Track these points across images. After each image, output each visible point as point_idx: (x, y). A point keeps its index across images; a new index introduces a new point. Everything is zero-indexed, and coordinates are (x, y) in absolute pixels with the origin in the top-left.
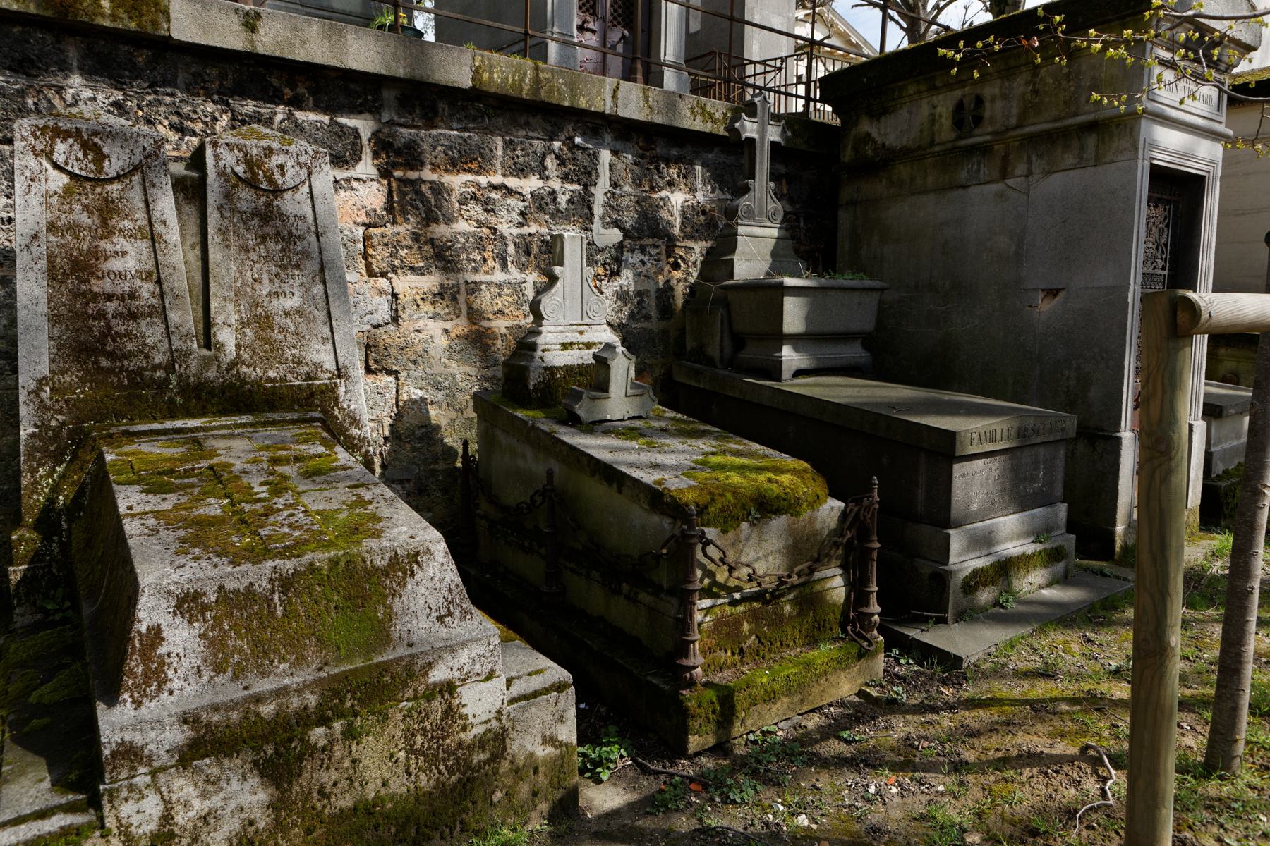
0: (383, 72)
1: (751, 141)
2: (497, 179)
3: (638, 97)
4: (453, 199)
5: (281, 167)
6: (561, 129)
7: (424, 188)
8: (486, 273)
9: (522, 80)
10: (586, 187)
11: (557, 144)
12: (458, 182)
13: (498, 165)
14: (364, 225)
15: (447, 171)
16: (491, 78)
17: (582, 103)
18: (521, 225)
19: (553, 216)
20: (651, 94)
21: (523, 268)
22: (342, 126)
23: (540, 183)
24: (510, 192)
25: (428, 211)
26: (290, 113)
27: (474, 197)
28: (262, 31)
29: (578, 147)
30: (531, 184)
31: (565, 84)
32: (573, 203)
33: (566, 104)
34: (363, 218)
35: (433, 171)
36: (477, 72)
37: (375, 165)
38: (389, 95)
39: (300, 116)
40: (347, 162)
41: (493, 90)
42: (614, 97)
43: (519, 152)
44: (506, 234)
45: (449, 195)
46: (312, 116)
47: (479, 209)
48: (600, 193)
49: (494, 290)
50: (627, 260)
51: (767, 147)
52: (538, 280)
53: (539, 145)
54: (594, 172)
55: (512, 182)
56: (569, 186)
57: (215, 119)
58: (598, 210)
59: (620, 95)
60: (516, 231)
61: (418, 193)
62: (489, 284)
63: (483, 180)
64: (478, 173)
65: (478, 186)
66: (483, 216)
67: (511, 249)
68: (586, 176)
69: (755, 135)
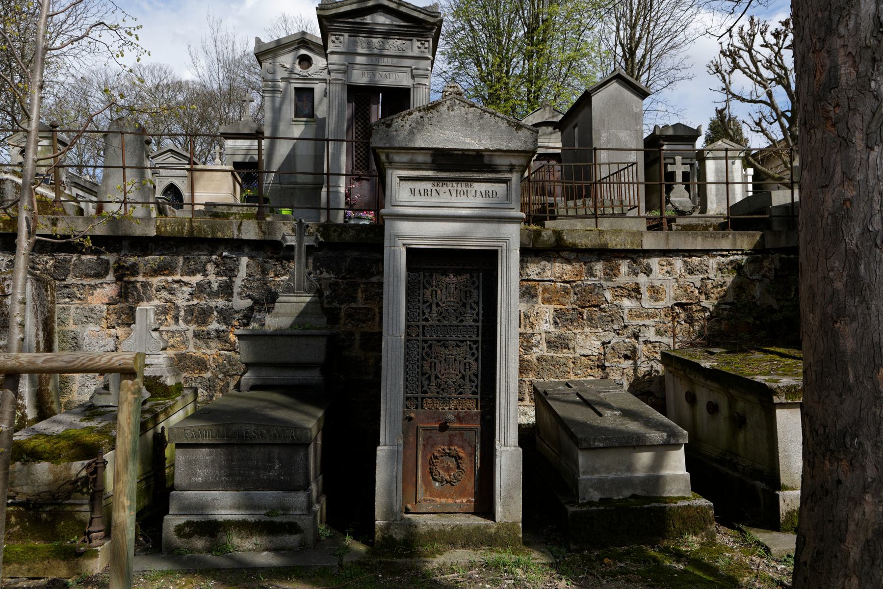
0: (111, 234)
1: (291, 248)
2: (177, 277)
3: (255, 227)
4: (153, 289)
5: (8, 285)
6: (217, 249)
7: (138, 285)
8: (167, 326)
9: (183, 228)
10: (230, 278)
11: (214, 257)
12: (156, 281)
13: (179, 270)
14: (107, 304)
15: (151, 276)
16: (166, 230)
17: (220, 235)
18: (188, 300)
19: (209, 295)
20: (263, 225)
21: (187, 322)
22: (102, 260)
23: (202, 278)
24: (186, 284)
25: (139, 295)
26: (79, 257)
27: (164, 288)
28: (59, 225)
29: (225, 257)
30: (199, 278)
31: (208, 227)
32: (221, 287)
33: (210, 237)
34: (107, 301)
35: (144, 276)
36: (158, 228)
37: (115, 276)
38: (125, 243)
39: (83, 257)
40: (102, 276)
41: (167, 235)
42: (239, 230)
43: (192, 263)
44: (180, 305)
45: (151, 287)
46: (89, 257)
47: (166, 293)
48: (238, 282)
49: (170, 334)
50: (255, 317)
51: (303, 249)
52: (196, 329)
53: (204, 258)
54: (236, 270)
55: (186, 279)
56: (220, 278)
57: (47, 263)
58: (236, 290)
59: (242, 228)
60: (185, 304)
61: (135, 288)
62: (167, 331)
63: (170, 279)
64: (168, 275)
65: (167, 282)
66: (168, 296)
67: (182, 313)
68: (231, 272)
69: (294, 243)
